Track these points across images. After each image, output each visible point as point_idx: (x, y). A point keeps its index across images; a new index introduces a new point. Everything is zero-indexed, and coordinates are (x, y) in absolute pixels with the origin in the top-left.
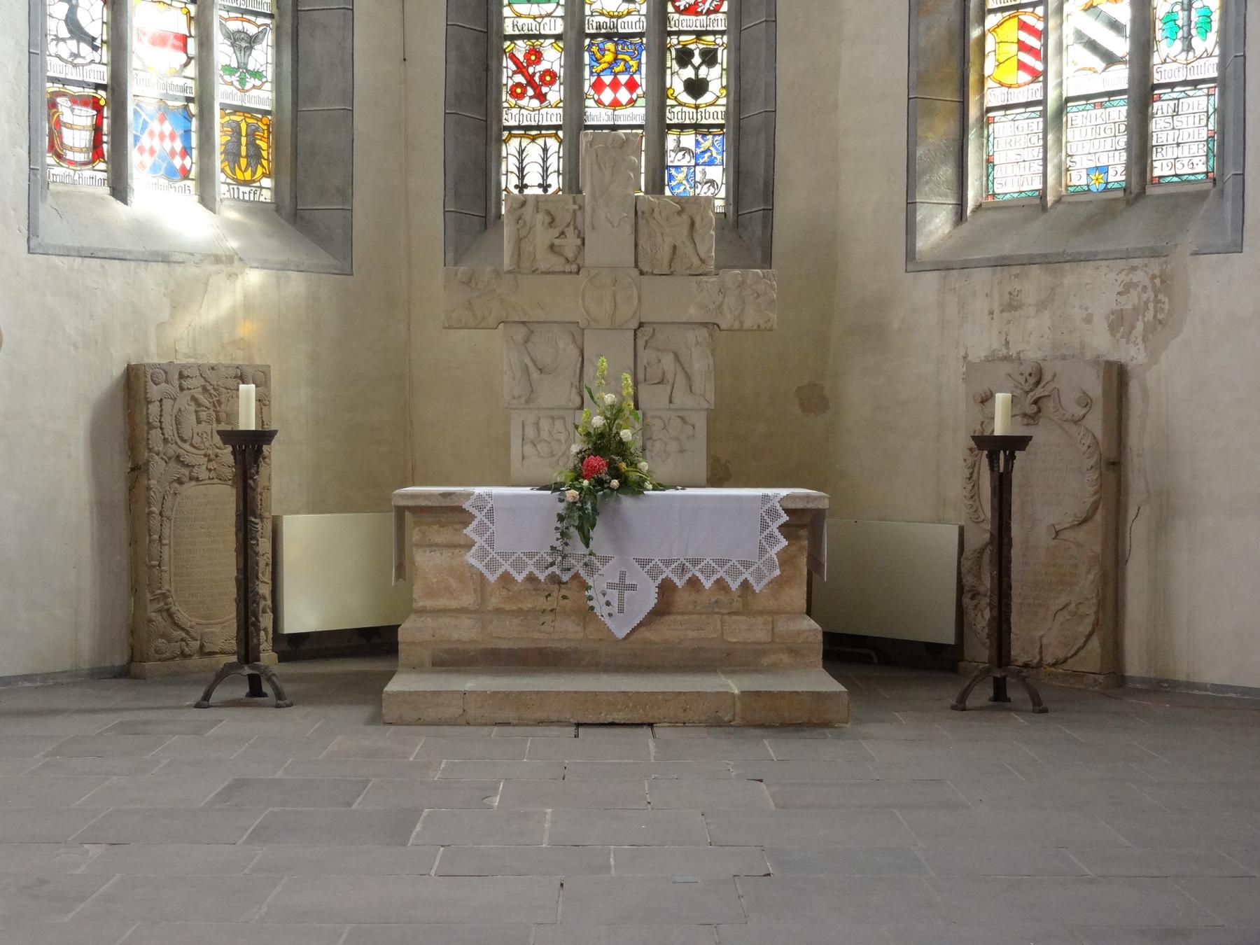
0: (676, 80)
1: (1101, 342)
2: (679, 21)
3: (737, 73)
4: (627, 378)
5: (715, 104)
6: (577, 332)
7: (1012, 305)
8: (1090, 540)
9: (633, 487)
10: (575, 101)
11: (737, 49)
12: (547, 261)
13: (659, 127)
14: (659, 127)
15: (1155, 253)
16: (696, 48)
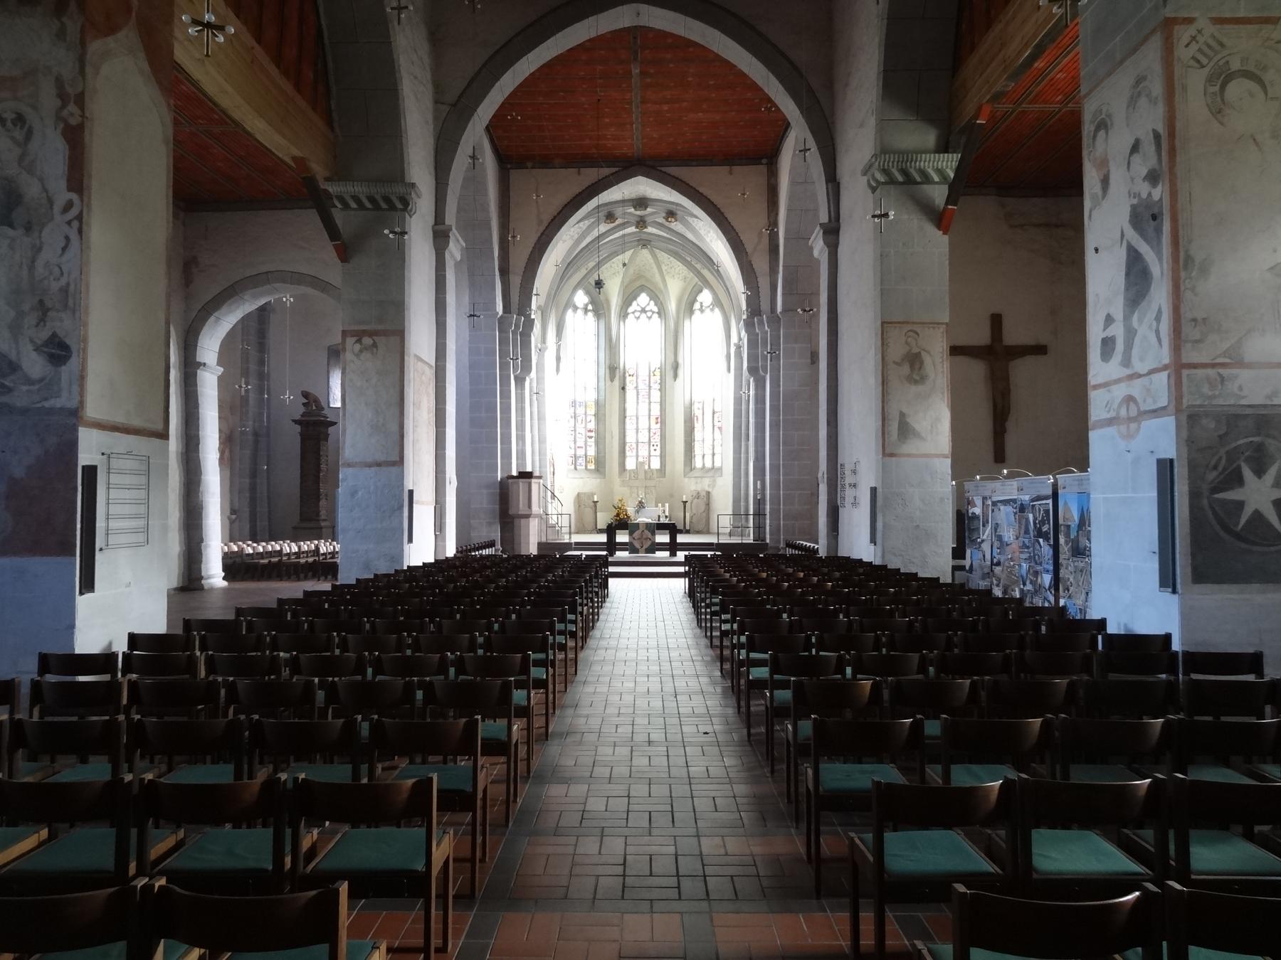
0: (652, 448)
1: (707, 489)
2: (652, 440)
3: (661, 448)
4: (644, 494)
5: (658, 452)
6: (637, 488)
7: (697, 483)
8: (704, 514)
9: (644, 507)
10: (637, 451)
11: (661, 444)
12: (633, 478)
13: (650, 456)
14: (650, 456)
15: (713, 477)
16: (655, 444)
